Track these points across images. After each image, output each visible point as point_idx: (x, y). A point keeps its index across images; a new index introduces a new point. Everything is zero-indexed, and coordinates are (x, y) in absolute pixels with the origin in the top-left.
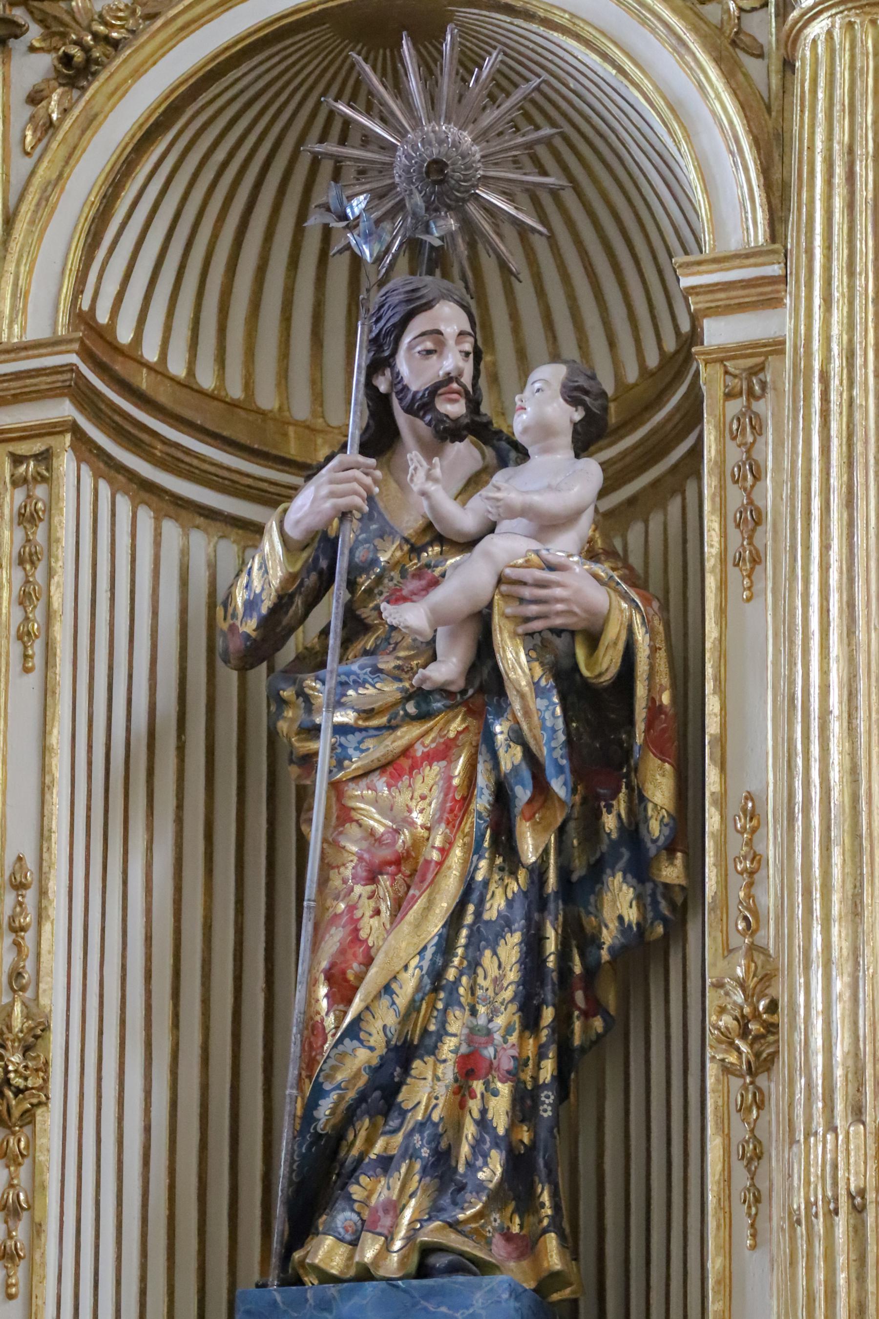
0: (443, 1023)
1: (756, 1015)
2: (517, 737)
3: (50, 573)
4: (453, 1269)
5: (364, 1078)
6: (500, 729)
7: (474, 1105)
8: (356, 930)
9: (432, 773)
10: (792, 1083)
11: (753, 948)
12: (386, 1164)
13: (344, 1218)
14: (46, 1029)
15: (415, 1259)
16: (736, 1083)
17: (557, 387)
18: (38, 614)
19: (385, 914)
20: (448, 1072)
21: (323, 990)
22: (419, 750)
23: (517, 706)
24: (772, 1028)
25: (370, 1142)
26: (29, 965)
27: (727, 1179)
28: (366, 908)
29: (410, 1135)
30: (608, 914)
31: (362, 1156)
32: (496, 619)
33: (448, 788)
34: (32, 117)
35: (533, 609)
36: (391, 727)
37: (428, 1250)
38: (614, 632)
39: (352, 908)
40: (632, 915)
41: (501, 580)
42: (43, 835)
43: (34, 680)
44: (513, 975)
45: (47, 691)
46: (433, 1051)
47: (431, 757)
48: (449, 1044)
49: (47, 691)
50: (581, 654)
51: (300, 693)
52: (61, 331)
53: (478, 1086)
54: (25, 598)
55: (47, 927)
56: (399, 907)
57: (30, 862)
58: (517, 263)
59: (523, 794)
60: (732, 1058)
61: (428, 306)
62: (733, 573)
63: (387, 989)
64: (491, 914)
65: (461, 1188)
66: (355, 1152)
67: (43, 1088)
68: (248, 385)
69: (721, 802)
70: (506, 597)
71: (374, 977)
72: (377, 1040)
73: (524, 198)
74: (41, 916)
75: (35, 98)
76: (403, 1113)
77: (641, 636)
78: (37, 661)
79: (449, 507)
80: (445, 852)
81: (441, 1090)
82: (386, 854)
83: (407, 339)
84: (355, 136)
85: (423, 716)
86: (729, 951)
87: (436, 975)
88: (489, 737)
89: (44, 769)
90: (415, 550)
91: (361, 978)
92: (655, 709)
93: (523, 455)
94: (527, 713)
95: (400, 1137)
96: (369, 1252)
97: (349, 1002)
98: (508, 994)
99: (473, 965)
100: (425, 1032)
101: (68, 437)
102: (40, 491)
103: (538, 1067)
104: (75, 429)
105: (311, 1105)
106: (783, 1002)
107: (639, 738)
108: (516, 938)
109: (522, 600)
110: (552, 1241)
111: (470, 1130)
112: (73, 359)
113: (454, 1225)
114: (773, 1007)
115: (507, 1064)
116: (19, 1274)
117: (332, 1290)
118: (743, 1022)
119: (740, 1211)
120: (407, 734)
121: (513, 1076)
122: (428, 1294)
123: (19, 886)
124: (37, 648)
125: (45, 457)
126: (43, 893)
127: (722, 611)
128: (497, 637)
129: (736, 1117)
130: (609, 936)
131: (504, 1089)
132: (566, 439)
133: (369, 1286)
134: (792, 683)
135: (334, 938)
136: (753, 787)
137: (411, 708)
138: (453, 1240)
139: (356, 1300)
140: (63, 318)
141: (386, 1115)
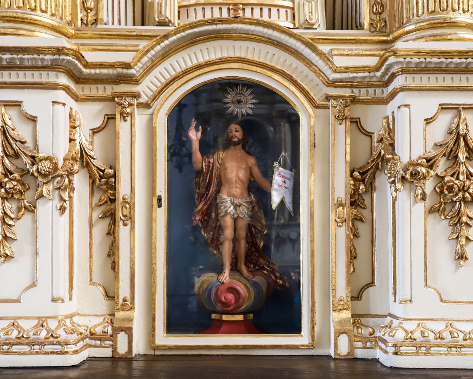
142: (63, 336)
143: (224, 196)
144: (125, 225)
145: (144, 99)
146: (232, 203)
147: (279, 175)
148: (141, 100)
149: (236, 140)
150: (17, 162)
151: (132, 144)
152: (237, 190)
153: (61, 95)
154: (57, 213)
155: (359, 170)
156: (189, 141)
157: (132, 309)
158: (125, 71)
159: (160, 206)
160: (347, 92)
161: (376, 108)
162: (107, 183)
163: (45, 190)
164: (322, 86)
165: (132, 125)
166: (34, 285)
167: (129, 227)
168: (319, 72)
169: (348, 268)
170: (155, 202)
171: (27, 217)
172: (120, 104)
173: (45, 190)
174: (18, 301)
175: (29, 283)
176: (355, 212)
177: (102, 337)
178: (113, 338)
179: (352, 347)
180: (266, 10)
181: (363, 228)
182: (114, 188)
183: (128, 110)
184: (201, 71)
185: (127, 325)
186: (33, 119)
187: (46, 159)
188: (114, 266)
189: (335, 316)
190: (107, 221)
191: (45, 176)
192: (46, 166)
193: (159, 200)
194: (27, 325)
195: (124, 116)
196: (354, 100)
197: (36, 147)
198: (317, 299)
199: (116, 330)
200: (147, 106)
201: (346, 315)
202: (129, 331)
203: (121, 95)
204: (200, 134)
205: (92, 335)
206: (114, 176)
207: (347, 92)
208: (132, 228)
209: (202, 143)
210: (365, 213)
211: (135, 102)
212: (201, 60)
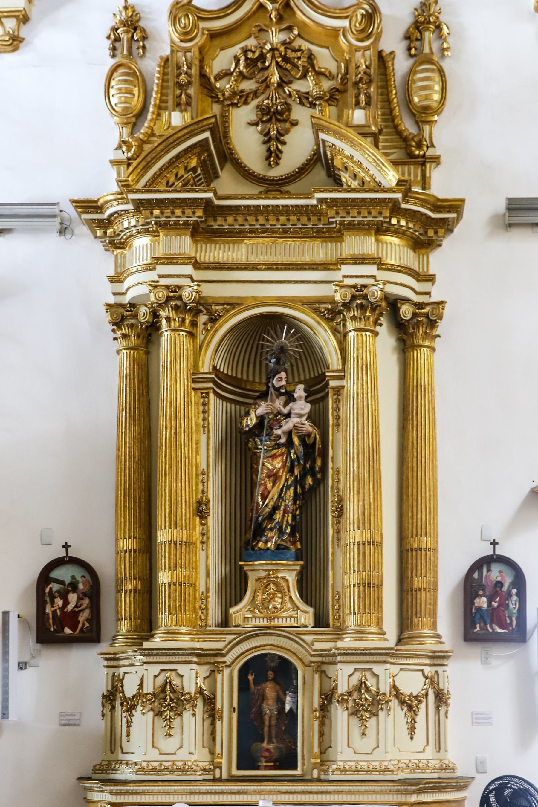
0: (281, 504)
1: (339, 507)
2: (295, 453)
3: (209, 416)
4: (284, 549)
5: (267, 514)
6: (292, 451)
7: (286, 518)
8: (266, 487)
9: (280, 459)
10: (346, 521)
11: (338, 496)
12: (271, 529)
13: (264, 539)
14: (209, 501)
15: (276, 547)
16: (335, 519)
17: (302, 389)
18: (206, 423)
19: (271, 484)
20: (282, 513)
21: (259, 498)
22: (277, 454)
23: (296, 448)
25: (267, 525)
26: (205, 489)
27: (333, 536)
28: (268, 483)
29: (275, 524)
30: (307, 483)
32: (293, 433)
33: (282, 461)
34: (204, 328)
35: (300, 431)
36: (273, 450)
38: (313, 435)
39: (265, 482)
40: (311, 483)
41: (294, 426)
42: (208, 465)
43: (205, 435)
44: (292, 495)
45: (208, 438)
46: (279, 509)
47: (280, 455)
48: (282, 508)
49: (208, 438)
50: (306, 439)
51: (254, 440)
52: (211, 371)
53: (286, 515)
54: (204, 420)
55: (209, 483)
57: (206, 470)
58: (294, 363)
59: (296, 463)
60: (334, 515)
61: (280, 373)
62: (335, 427)
63: (272, 498)
64: (289, 484)
65: (284, 533)
66: (264, 526)
67: (209, 512)
68: (236, 374)
69: (332, 468)
70: (295, 429)
71: (270, 495)
72: (270, 507)
73: (297, 353)
74: (208, 480)
75: (205, 324)
76: (274, 520)
77: (318, 436)
78: (206, 432)
79: (283, 409)
80: (282, 473)
81: (281, 516)
82: (272, 474)
83: (276, 378)
85: (278, 448)
86: (334, 496)
88: (290, 453)
89: (208, 452)
90: (276, 416)
92: (319, 448)
93: (295, 400)
94: (298, 449)
95: (273, 524)
96: (269, 544)
97: (266, 500)
98: (291, 498)
99: (286, 492)
100: (278, 506)
101: (212, 390)
102: (206, 399)
103: (296, 512)
104: (213, 389)
105: (258, 518)
106: (345, 506)
107: (316, 454)
108: (292, 488)
109: (298, 430)
110: (299, 543)
111: (285, 523)
112: (213, 376)
113: (283, 540)
114: (342, 506)
115: (291, 511)
116: (205, 546)
117: (262, 551)
118: (337, 508)
119: (335, 541)
120: (275, 451)
121: (292, 513)
122: (280, 553)
123: (203, 474)
124: (206, 429)
125: (207, 393)
126: (208, 476)
127: (333, 434)
128: (293, 436)
129: (335, 525)
130: (307, 486)
131: (290, 515)
132: (304, 399)
133: (269, 551)
134: (347, 450)
135: (262, 488)
136: (338, 466)
137: (276, 447)
138: (283, 543)
139: (266, 554)
140: (211, 367)
141: (271, 521)
142: (195, 768)
143: (265, 705)
144: (219, 720)
145: (228, 663)
146: (268, 709)
147: (290, 697)
148: (227, 664)
149: (270, 679)
150: (176, 695)
151: (223, 684)
152: (271, 702)
153: (194, 666)
154: (191, 716)
155: (324, 694)
156: (248, 681)
157: (222, 758)
158: (220, 652)
159: (234, 712)
160: (319, 659)
161: (332, 666)
162: (211, 702)
163: (187, 706)
164: (308, 656)
165: (223, 676)
166: (181, 747)
167: (220, 722)
168: (307, 651)
169: (319, 739)
170: (232, 710)
171: (178, 719)
172: (217, 666)
173: (187, 706)
174: (175, 754)
175: (179, 746)
176: (322, 713)
177: (209, 770)
178: (213, 771)
179: (319, 775)
180: (284, 619)
181: (327, 721)
182: (214, 704)
183: (221, 669)
184: (253, 650)
185: (220, 765)
186: (182, 676)
187: (188, 693)
188: (214, 739)
189: (313, 761)
190: (211, 719)
191: (187, 701)
192: (187, 697)
193: (234, 709)
194: (180, 764)
195: (219, 671)
196: (323, 663)
197: (183, 688)
198: (305, 754)
199: (215, 768)
200: (229, 666)
201: (318, 760)
202: (220, 768)
203: (219, 663)
204: (253, 677)
205: (204, 770)
206: (214, 698)
207: (319, 659)
208: (222, 722)
209: (254, 680)
210: (328, 714)
211: (224, 665)
212: (254, 645)
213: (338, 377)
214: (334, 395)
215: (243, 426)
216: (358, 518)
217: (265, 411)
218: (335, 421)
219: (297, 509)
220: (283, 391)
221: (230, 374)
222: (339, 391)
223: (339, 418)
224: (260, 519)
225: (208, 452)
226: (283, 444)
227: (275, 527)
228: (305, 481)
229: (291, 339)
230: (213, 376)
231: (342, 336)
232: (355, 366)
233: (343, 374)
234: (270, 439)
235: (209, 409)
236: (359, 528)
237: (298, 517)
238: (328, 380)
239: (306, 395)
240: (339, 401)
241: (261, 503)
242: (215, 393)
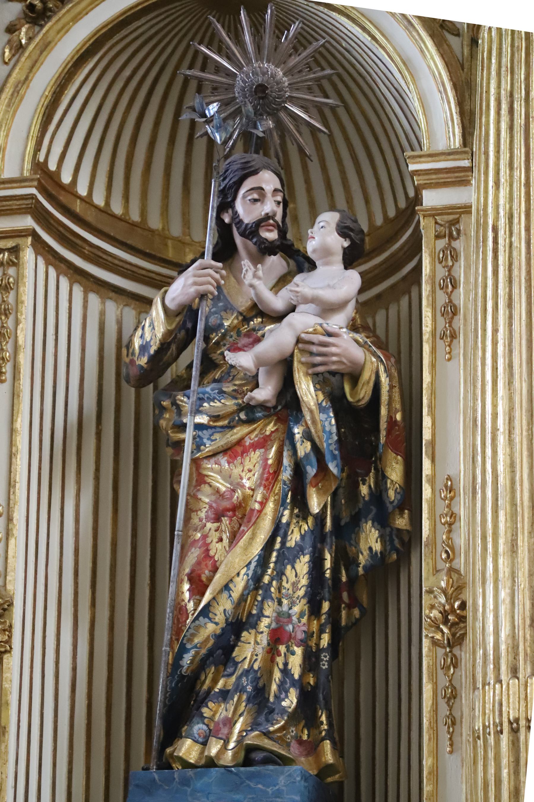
0: (261, 609)
1: (453, 611)
2: (308, 436)
4: (266, 761)
5: (212, 642)
6: (298, 431)
7: (280, 660)
8: (208, 550)
9: (256, 456)
11: (451, 571)
12: (225, 695)
13: (198, 728)
16: (441, 652)
17: (334, 226)
19: (226, 541)
20: (264, 639)
21: (186, 586)
22: (248, 442)
23: (308, 417)
24: (463, 619)
25: (215, 681)
28: (214, 537)
29: (239, 678)
31: (210, 689)
32: (296, 364)
33: (265, 466)
34: (9, 42)
35: (319, 359)
36: (230, 427)
37: (251, 749)
38: (367, 375)
39: (205, 537)
41: (299, 340)
46: (255, 626)
47: (255, 446)
48: (265, 622)
50: (347, 388)
51: (174, 403)
53: (282, 649)
56: (234, 537)
59: (311, 471)
60: (438, 636)
61: (255, 172)
62: (440, 344)
63: (226, 587)
65: (272, 711)
66: (205, 687)
69: (432, 481)
70: (302, 351)
71: (219, 579)
72: (220, 618)
76: (236, 664)
77: (384, 379)
80: (263, 504)
81: (260, 650)
82: (226, 504)
84: (211, 66)
85: (250, 421)
87: (257, 579)
88: (291, 436)
90: (246, 320)
91: (210, 579)
93: (312, 266)
95: (233, 679)
96: (214, 749)
97: (203, 594)
99: (280, 574)
100: (250, 614)
105: (179, 656)
107: (383, 440)
109: (311, 354)
111: (277, 675)
113: (267, 734)
114: (463, 606)
118: (445, 614)
119: (443, 730)
120: (240, 432)
122: (251, 776)
127: (433, 366)
128: (296, 375)
129: (440, 672)
132: (339, 257)
136: (451, 472)
137: (243, 416)
138: (267, 743)
141: (225, 665)
213: (451, 177)
214: (438, 237)
215: (133, 354)
216: (513, 636)
217: (192, 290)
218: (441, 322)
219: (321, 631)
220: (272, 235)
221: (117, 209)
222: (457, 221)
223: (455, 312)
224: (187, 659)
225: (11, 443)
226: (262, 406)
227: (239, 688)
228: (357, 543)
229: (294, 61)
230: (34, 191)
231: (467, 41)
232: (504, 126)
233: (466, 163)
234: (221, 392)
235: (18, 301)
236: (514, 672)
237: (325, 658)
238: (418, 191)
239: (346, 244)
240: (455, 258)
241: (191, 606)
242: (38, 241)
